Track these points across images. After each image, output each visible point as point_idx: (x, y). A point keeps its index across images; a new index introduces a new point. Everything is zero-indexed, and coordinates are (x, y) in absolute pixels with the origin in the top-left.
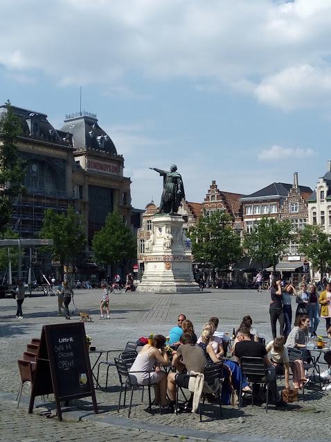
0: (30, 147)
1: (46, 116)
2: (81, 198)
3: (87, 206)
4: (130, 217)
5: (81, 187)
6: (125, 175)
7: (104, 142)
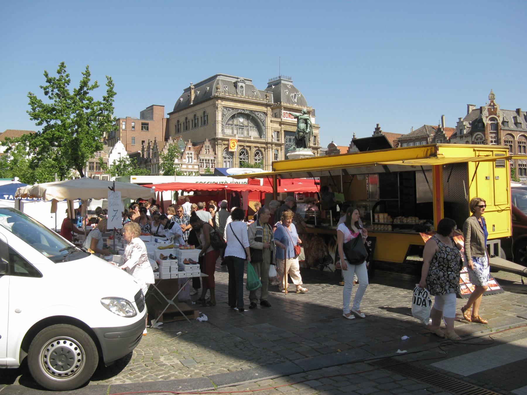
5: (278, 132)
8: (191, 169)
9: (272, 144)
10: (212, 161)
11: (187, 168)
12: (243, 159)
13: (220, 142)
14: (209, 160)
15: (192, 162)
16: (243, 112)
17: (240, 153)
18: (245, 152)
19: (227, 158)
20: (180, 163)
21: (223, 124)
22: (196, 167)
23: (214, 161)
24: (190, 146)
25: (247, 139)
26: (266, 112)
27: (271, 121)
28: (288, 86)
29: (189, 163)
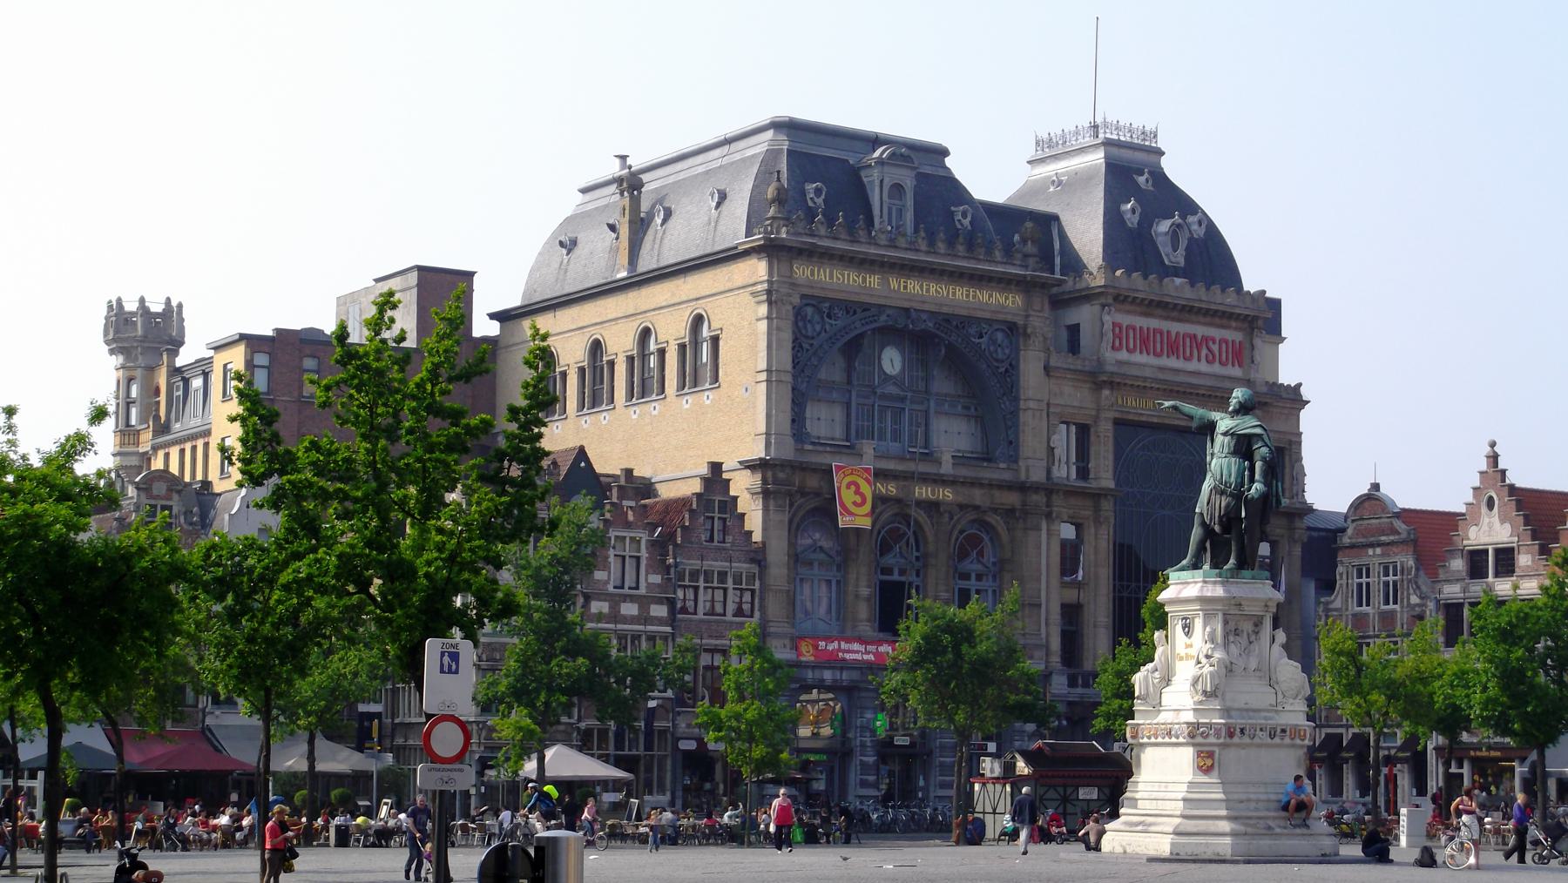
0: (874, 281)
1: (944, 152)
2: (1083, 473)
3: (1107, 506)
4: (1298, 550)
5: (1083, 432)
6: (1286, 377)
7: (1183, 244)
9: (1050, 489)
10: (738, 580)
11: (615, 617)
12: (896, 572)
14: (723, 576)
15: (637, 588)
17: (883, 538)
18: (910, 533)
22: (660, 611)
23: (751, 578)
25: (924, 468)
26: (1021, 322)
27: (1047, 369)
28: (1141, 180)
29: (626, 591)
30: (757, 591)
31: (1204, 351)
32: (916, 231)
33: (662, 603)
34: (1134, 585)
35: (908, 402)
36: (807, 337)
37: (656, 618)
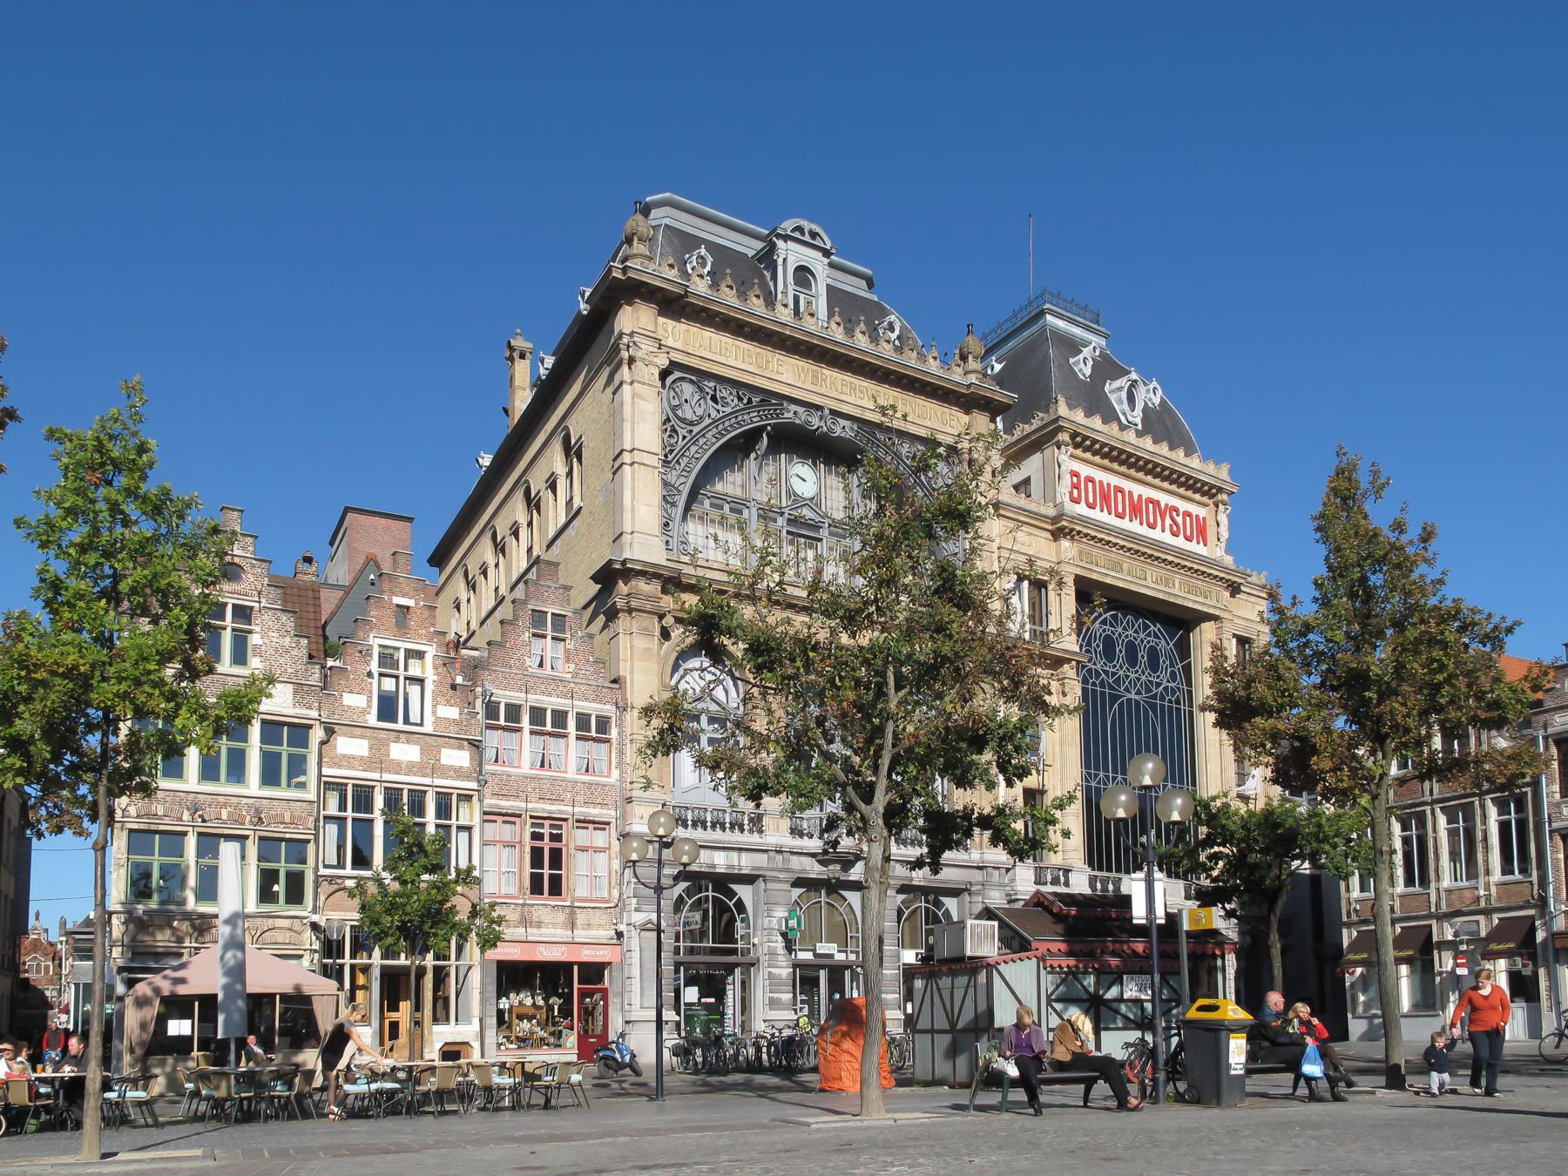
3: (1068, 670)
8: (411, 768)
10: (583, 721)
11: (379, 760)
13: (648, 598)
15: (421, 724)
16: (815, 422)
19: (704, 719)
20: (314, 714)
21: (672, 477)
22: (459, 758)
24: (410, 602)
30: (614, 742)
31: (1168, 521)
32: (831, 315)
33: (461, 748)
34: (1102, 774)
35: (824, 533)
36: (682, 420)
37: (451, 768)
